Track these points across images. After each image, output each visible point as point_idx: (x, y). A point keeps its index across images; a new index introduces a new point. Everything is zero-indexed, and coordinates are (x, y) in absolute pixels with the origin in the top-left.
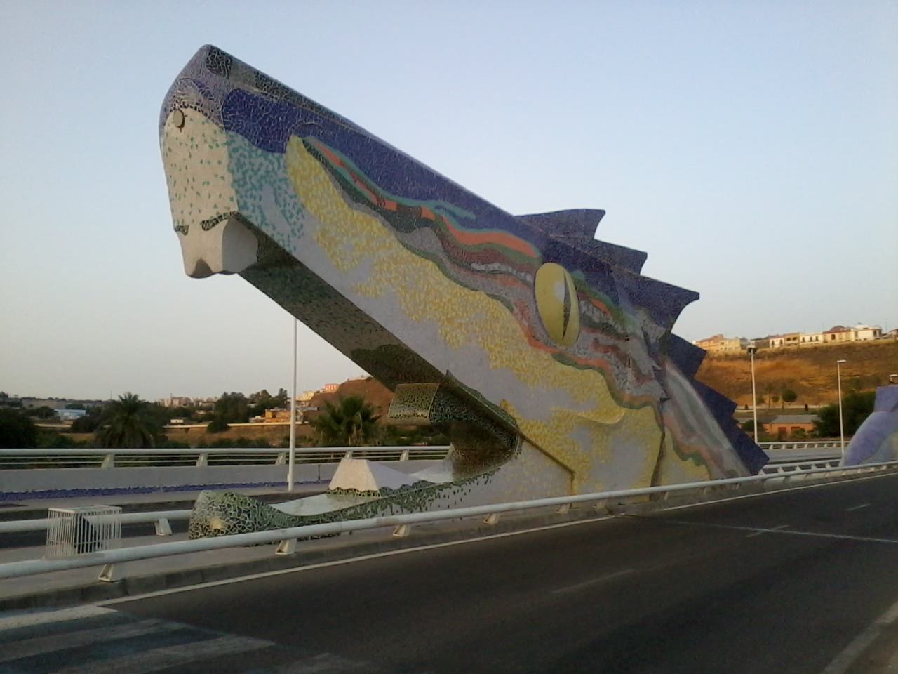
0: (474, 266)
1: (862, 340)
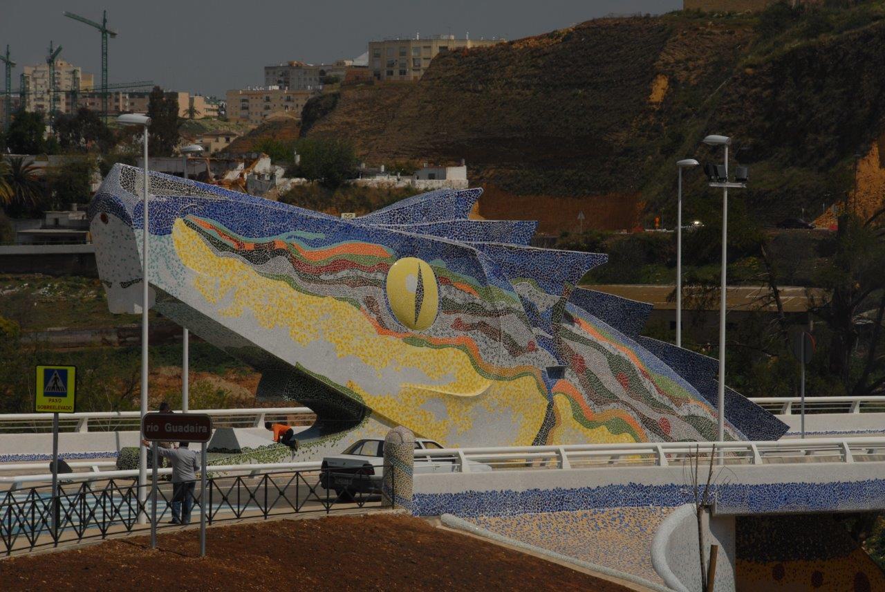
0: (323, 277)
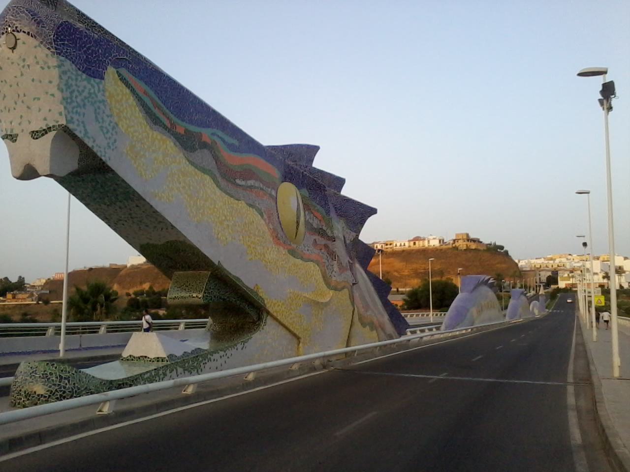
0: (238, 181)
1: (432, 245)
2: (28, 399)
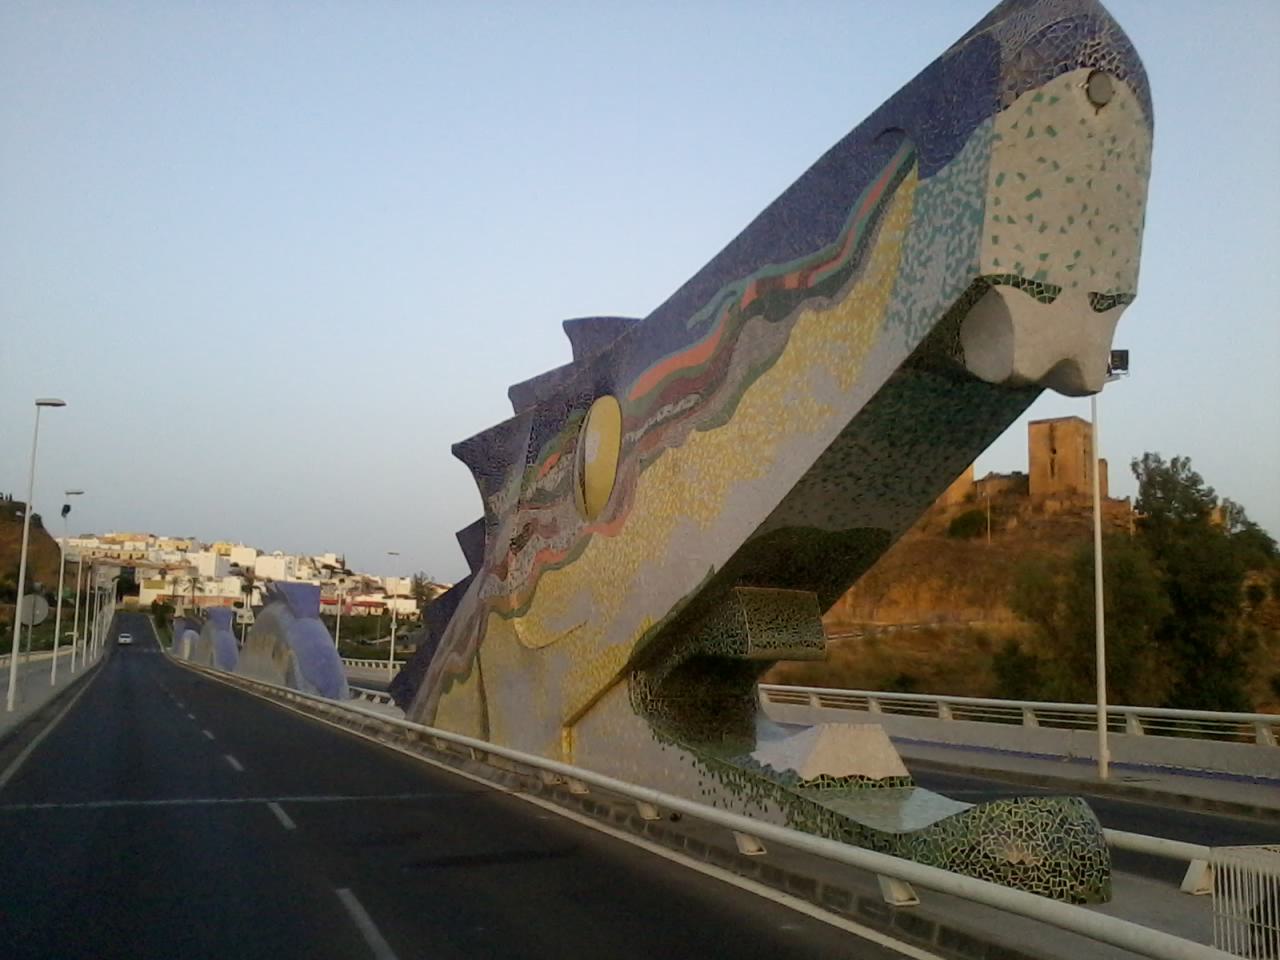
2: (1082, 883)
